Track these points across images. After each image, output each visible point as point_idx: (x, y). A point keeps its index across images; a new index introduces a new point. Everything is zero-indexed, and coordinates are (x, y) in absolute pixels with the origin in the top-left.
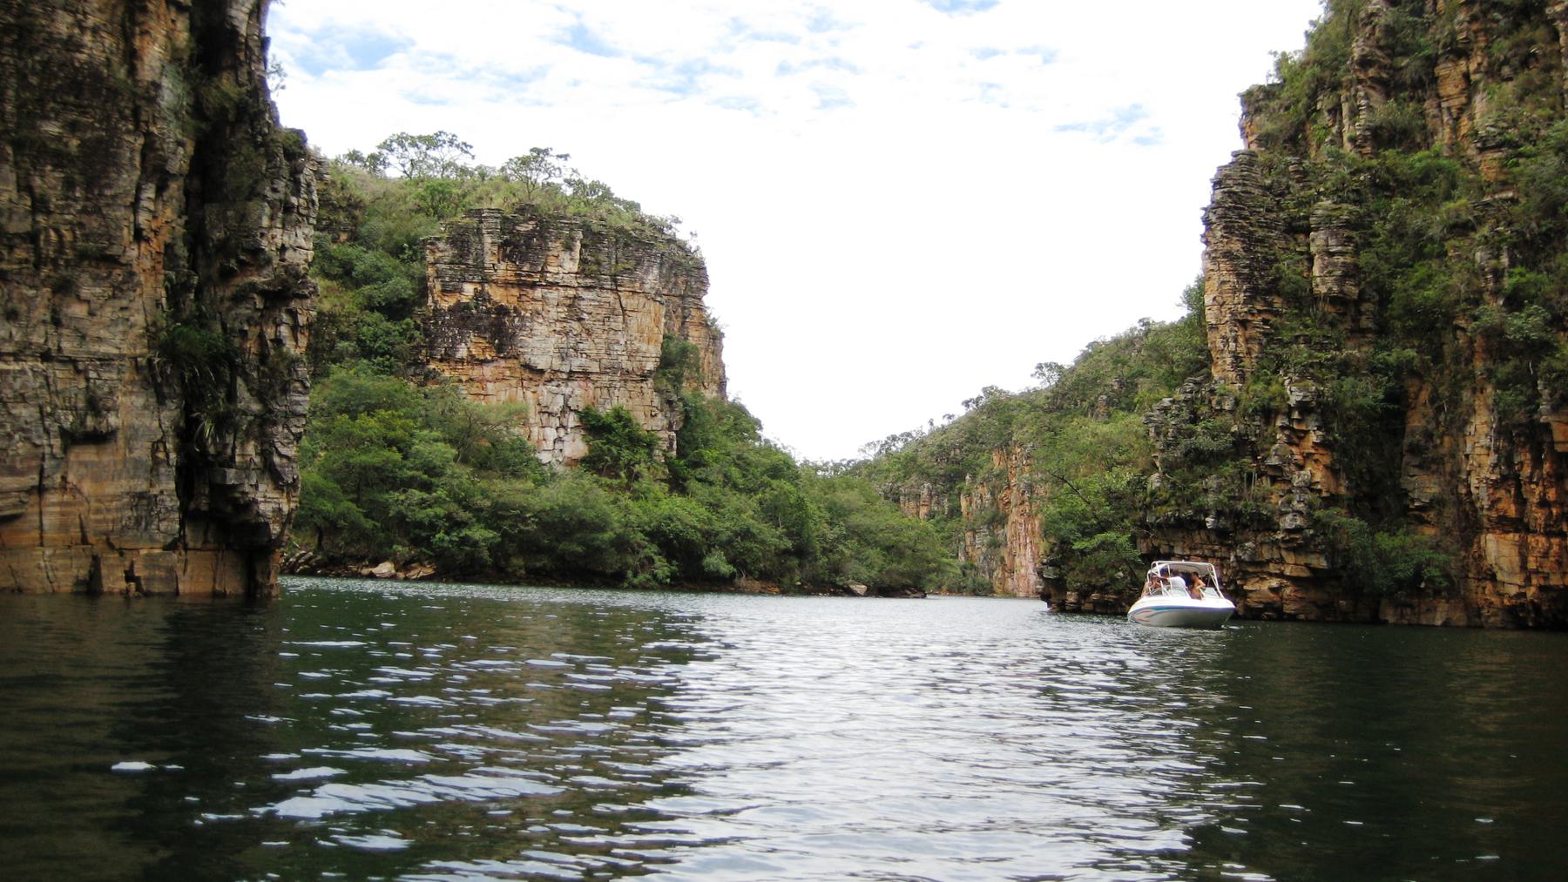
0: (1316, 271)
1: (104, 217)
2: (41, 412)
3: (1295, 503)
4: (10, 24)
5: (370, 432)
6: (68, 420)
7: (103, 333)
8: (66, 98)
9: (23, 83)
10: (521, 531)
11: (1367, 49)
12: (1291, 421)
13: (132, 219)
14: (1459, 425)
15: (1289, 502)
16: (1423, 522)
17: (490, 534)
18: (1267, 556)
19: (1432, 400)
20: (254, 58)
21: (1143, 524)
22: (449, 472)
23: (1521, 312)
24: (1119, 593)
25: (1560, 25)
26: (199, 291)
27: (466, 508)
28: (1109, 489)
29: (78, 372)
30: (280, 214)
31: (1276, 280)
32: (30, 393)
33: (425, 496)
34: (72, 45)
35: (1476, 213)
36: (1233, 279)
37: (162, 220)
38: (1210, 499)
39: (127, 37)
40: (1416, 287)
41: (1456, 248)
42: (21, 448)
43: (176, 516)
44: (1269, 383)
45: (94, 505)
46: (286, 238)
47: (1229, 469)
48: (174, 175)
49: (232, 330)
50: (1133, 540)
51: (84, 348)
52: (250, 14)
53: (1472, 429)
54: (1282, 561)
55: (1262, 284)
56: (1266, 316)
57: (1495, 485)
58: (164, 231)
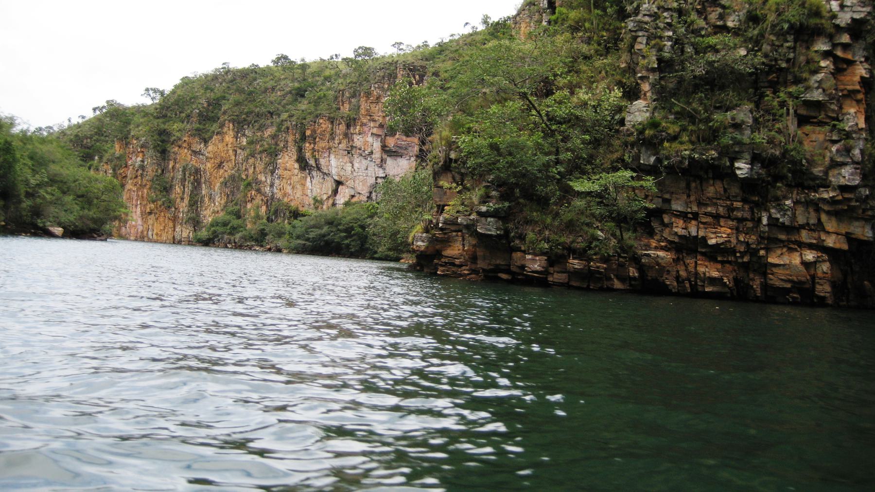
18: (801, 220)
54: (820, 227)
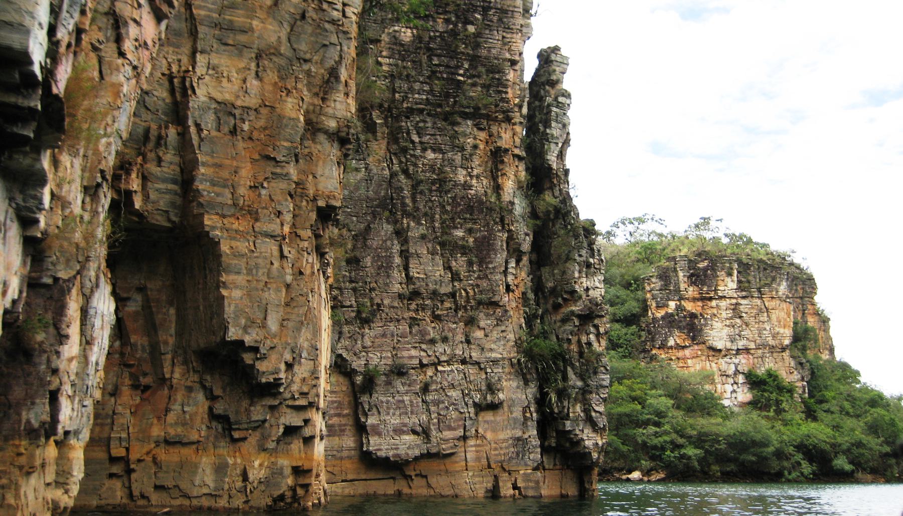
1: (489, 280)
2: (463, 394)
4: (435, 179)
5: (622, 394)
6: (477, 398)
7: (493, 346)
8: (465, 216)
9: (444, 211)
10: (716, 449)
13: (504, 280)
17: (698, 451)
20: (562, 181)
22: (670, 415)
26: (542, 318)
27: (682, 436)
29: (481, 369)
30: (584, 269)
32: (456, 383)
33: (658, 430)
34: (467, 186)
37: (520, 279)
39: (494, 178)
42: (454, 415)
43: (539, 450)
45: (493, 445)
46: (588, 283)
48: (525, 253)
49: (562, 339)
51: (483, 356)
52: (557, 157)
58: (521, 285)
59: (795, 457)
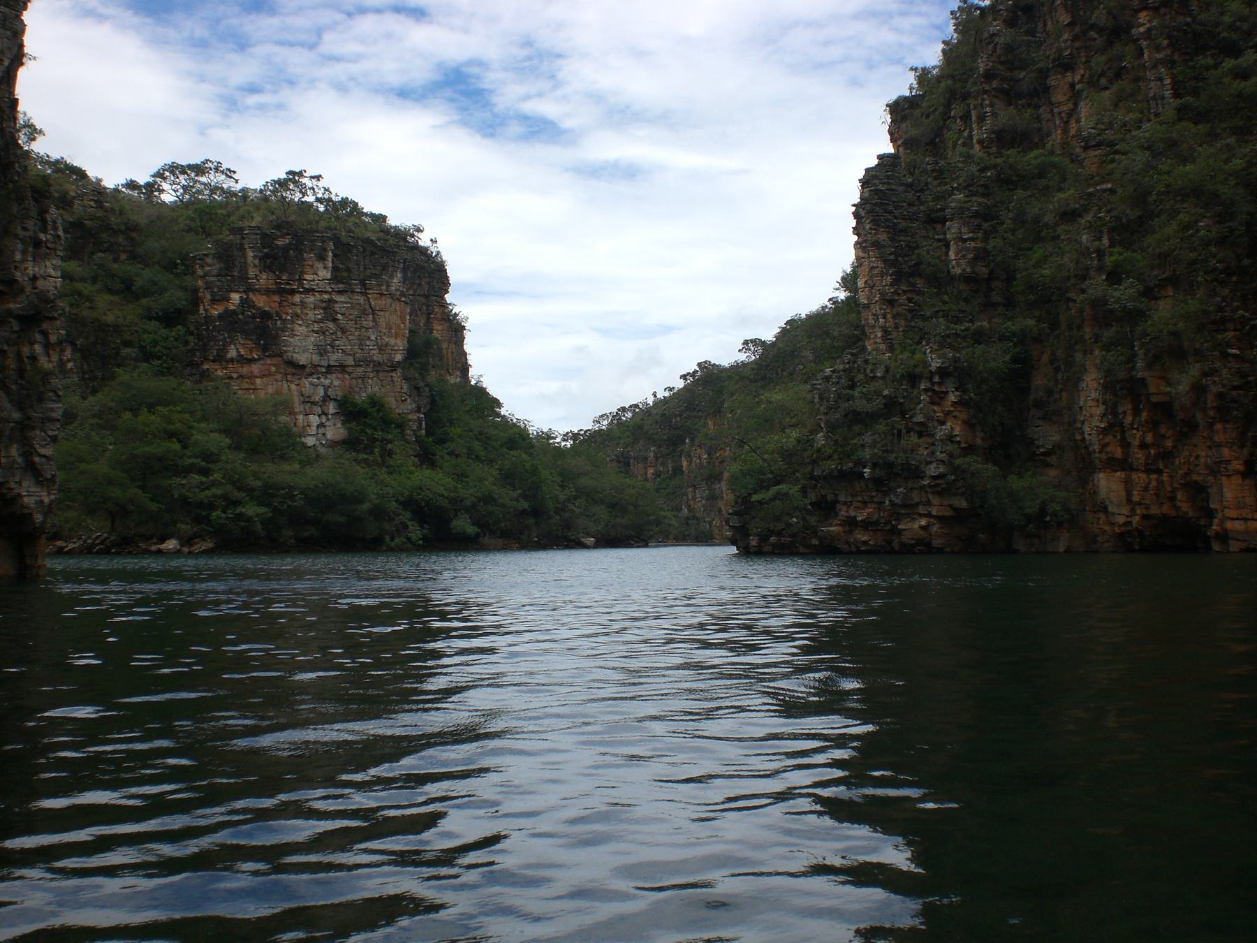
0: (952, 255)
3: (938, 453)
10: (289, 507)
11: (991, 64)
12: (933, 384)
14: (1074, 383)
15: (933, 453)
16: (1049, 465)
17: (262, 510)
18: (916, 499)
19: (1051, 362)
20: (5, 117)
21: (812, 477)
22: (223, 458)
23: (1120, 285)
24: (793, 536)
25: (1144, 43)
27: (239, 489)
28: (782, 448)
30: (31, 249)
31: (918, 264)
33: (204, 479)
35: (1082, 202)
36: (880, 264)
38: (867, 454)
40: (1035, 266)
41: (1067, 232)
44: (913, 353)
46: (37, 269)
47: (881, 427)
50: (804, 491)
53: (1084, 385)
54: (929, 503)
55: (905, 268)
56: (910, 295)
57: (1104, 431)
59: (401, 517)
